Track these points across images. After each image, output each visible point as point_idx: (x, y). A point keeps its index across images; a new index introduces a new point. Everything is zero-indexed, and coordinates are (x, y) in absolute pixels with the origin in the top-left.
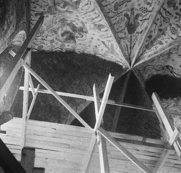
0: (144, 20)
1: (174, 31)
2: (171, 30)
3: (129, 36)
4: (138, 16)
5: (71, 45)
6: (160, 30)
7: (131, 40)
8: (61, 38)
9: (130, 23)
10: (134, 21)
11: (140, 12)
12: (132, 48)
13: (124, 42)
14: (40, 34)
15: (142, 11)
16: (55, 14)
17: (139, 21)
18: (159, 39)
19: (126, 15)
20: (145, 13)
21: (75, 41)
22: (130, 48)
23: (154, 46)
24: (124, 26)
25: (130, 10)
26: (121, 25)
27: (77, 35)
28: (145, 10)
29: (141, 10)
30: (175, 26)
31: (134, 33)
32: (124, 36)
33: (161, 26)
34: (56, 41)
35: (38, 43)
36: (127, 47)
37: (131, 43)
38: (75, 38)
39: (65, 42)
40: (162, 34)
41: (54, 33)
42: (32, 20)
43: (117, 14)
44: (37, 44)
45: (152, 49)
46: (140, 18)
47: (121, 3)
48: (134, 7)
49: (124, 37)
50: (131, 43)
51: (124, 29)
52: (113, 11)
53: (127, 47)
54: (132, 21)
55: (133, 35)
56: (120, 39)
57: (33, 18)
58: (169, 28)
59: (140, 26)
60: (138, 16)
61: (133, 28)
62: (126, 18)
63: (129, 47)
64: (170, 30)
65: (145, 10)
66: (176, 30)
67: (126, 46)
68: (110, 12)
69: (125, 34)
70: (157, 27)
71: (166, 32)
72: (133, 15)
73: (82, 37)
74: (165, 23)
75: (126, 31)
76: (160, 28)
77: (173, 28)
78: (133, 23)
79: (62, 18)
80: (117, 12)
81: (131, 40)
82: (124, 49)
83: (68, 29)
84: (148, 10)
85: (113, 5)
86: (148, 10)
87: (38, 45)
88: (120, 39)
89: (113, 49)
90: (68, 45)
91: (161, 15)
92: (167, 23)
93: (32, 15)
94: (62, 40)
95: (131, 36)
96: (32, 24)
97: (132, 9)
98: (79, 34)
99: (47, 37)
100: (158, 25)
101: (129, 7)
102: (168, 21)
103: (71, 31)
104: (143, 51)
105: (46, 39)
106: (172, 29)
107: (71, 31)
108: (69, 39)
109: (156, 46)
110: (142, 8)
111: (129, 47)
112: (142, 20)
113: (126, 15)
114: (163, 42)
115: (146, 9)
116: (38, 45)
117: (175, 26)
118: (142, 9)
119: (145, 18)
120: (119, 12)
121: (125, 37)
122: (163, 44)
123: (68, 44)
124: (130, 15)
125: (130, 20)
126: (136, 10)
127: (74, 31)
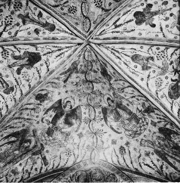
0: (17, 49)
1: (18, 5)
2: (19, 9)
3: (44, 58)
4: (15, 58)
5: (83, 109)
6: (24, 23)
7: (49, 53)
8: (75, 126)
9: (27, 63)
10: (24, 59)
11: (10, 57)
12: (59, 48)
13: (53, 62)
14: (71, 153)
15: (8, 56)
16: (42, 145)
17: (22, 53)
18: (36, 18)
19: (19, 72)
20: (8, 52)
21: (77, 107)
22: (60, 50)
23: (48, 21)
24: (33, 69)
25: (11, 69)
26: (31, 75)
27: (67, 109)
28: (5, 54)
29: (7, 57)
30: (12, 7)
31: (39, 53)
32: (45, 66)
33: (18, 24)
34: (80, 131)
35: (83, 151)
36: (59, 55)
37: (52, 52)
38: (73, 108)
39: (80, 119)
40: (29, 17)
41: (69, 137)
42: (53, 168)
43: (18, 87)
44: (85, 154)
45: (52, 23)
46: (17, 54)
47: (4, 85)
48: (6, 65)
49: (46, 65)
50: (52, 52)
51: (36, 69)
52: (13, 93)
53: (59, 55)
54: (24, 62)
55: (42, 54)
56: (48, 70)
57: (51, 167)
58: (18, 13)
59: (27, 50)
60: (15, 58)
61: (33, 57)
62: (22, 71)
63: (58, 53)
64: (19, 10)
65: (5, 54)
66: (16, 3)
67: (59, 58)
68: (15, 98)
69: (41, 65)
70: (21, 29)
71: (23, 14)
72: (16, 62)
73: (70, 102)
74: (13, 20)
75: (37, 65)
76: (21, 24)
77: (14, 8)
78: (26, 59)
79: (46, 135)
80: (15, 86)
81: (49, 53)
82: (62, 59)
83: (61, 122)
84: (3, 50)
85: (5, 96)
86: (3, 50)
87: (85, 152)
88: (48, 70)
89: (69, 70)
90: (85, 113)
91: (4, 33)
92: (12, 19)
93: (47, 170)
94: (78, 123)
95: (44, 55)
96: (58, 166)
97: (10, 66)
98: (65, 107)
99: (75, 144)
100: (17, 28)
101: (8, 72)
102: (9, 18)
103: (63, 117)
104: (60, 32)
105: (77, 144)
106: (16, 9)
107: (63, 117)
108: (76, 115)
109: (46, 19)
110: (3, 57)
111: (58, 53)
112: (19, 51)
113: (19, 72)
114: (37, 13)
115: (2, 53)
116: (85, 152)
117: (12, 7)
118: (5, 57)
119: (14, 49)
120: (16, 84)
121: (46, 64)
122: (40, 12)
123: (83, 113)
124: (18, 66)
125: (24, 65)
126: (9, 62)
127: (62, 114)
